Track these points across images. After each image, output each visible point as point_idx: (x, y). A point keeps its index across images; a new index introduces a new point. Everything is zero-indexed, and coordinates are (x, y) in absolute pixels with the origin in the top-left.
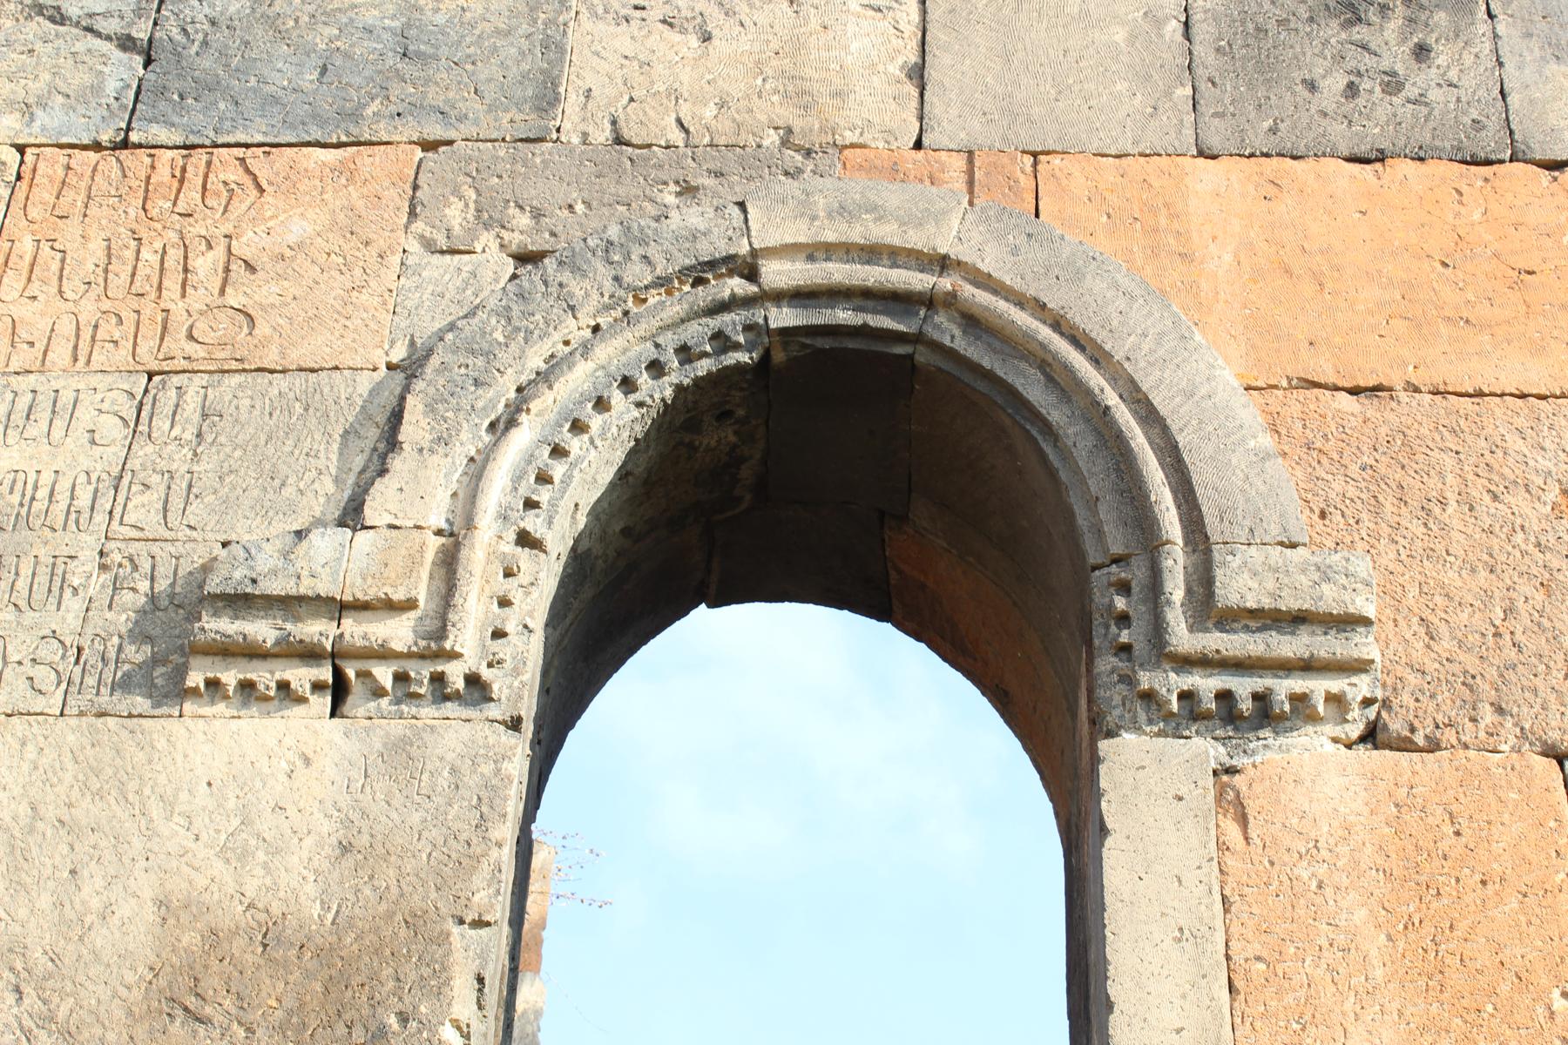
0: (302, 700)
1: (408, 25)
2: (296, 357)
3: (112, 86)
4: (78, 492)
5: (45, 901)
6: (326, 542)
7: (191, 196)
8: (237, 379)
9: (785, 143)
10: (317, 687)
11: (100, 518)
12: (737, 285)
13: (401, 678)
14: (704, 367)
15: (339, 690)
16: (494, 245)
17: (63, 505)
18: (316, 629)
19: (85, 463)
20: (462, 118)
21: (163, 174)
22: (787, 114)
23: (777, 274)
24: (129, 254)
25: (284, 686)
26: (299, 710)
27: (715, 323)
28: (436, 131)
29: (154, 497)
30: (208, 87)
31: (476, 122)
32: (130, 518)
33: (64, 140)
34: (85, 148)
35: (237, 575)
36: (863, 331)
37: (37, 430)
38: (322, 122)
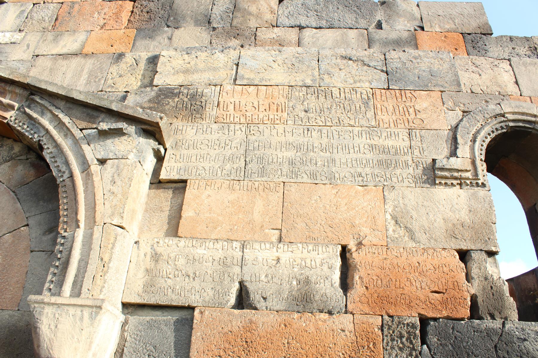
0: (455, 186)
1: (430, 70)
2: (433, 127)
3: (383, 79)
5: (424, 218)
6: (453, 159)
7: (404, 98)
8: (424, 131)
9: (499, 94)
10: (458, 184)
11: (410, 154)
12: (503, 119)
13: (471, 183)
14: (499, 132)
16: (458, 110)
18: (456, 174)
21: (398, 95)
22: (499, 89)
23: (510, 117)
24: (397, 108)
25: (452, 184)
26: (454, 188)
27: (501, 124)
28: (442, 89)
29: (418, 150)
35: (441, 164)
36: (525, 127)
37: (393, 138)
38: (422, 87)
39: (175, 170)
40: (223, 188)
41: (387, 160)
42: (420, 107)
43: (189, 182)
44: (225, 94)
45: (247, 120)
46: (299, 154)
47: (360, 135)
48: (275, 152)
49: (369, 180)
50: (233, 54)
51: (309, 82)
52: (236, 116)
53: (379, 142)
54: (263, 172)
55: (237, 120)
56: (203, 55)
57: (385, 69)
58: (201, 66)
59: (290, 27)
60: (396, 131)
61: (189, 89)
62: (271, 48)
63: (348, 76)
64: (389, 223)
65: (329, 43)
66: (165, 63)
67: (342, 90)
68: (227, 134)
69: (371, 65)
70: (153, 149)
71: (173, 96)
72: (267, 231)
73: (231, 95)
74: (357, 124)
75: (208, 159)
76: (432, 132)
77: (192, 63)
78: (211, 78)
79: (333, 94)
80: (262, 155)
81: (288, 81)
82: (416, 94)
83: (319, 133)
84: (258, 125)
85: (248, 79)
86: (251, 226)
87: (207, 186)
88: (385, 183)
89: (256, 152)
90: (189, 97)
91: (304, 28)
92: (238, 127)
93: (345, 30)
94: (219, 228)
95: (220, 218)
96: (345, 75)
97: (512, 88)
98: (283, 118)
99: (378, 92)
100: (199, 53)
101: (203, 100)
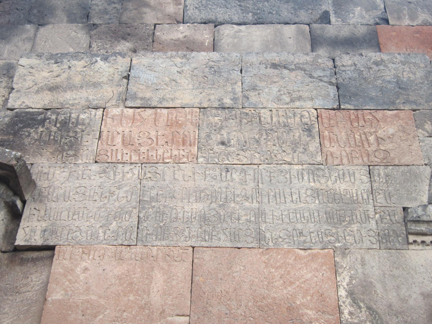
2: (403, 162)
3: (332, 95)
4: (363, 194)
7: (362, 123)
8: (391, 167)
11: (371, 201)
17: (361, 198)
19: (363, 188)
20: (420, 104)
21: (353, 117)
28: (415, 107)
30: (355, 95)
31: (424, 105)
32: (379, 201)
33: (326, 107)
34: (331, 109)
35: (415, 215)
37: (347, 179)
38: (388, 104)
39: (38, 232)
40: (106, 257)
41: (339, 211)
42: (385, 133)
43: (57, 249)
44: (109, 121)
45: (141, 158)
46: (214, 205)
47: (300, 177)
48: (180, 204)
49: (313, 241)
50: (122, 63)
51: (228, 101)
52: (125, 152)
53: (327, 186)
54: (163, 232)
55: (126, 158)
56: (79, 65)
57: (334, 80)
58: (77, 80)
59: (202, 23)
60: (352, 168)
61: (58, 114)
62: (174, 53)
63: (282, 93)
64: (344, 303)
65: (257, 45)
66: (25, 75)
67: (274, 111)
68: (112, 178)
69: (315, 75)
70: (6, 203)
71: (35, 124)
72: (169, 318)
73: (119, 124)
74: (296, 160)
75: (85, 216)
76: (402, 168)
77: (64, 76)
78: (91, 97)
79: (262, 119)
80: (161, 207)
81: (198, 100)
82: (379, 115)
83: (243, 175)
84: (157, 165)
85: (142, 99)
86: (147, 311)
87: (84, 255)
88: (337, 245)
89: (153, 204)
90: (58, 125)
91: (221, 24)
92: (127, 168)
93: (279, 26)
94: (101, 317)
95: (102, 302)
96: (279, 91)
98: (192, 155)
99: (325, 114)
100: (73, 62)
101: (78, 130)
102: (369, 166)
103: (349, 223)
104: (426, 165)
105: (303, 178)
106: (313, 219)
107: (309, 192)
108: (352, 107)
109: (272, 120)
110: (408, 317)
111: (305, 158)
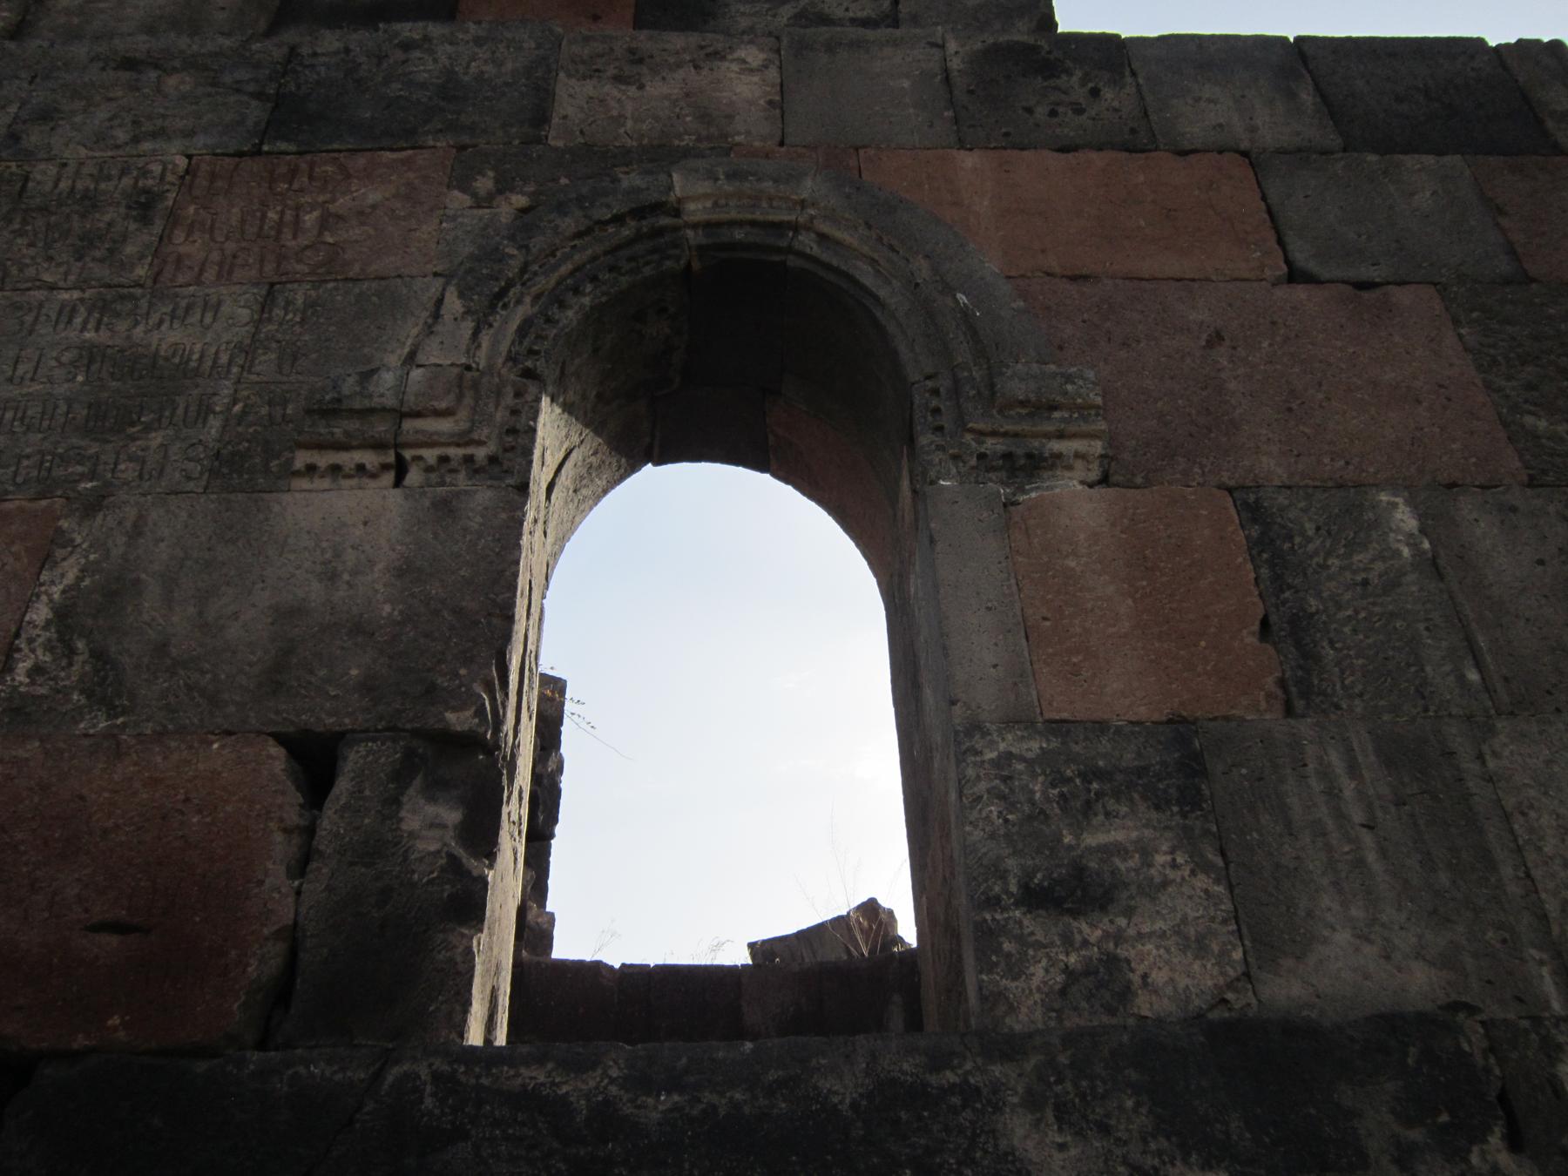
0: (374, 476)
10: (385, 467)
15: (401, 469)
18: (381, 428)
26: (372, 484)
47: (64, 319)
53: (128, 338)
63: (116, 122)
79: (30, 184)
82: (361, 161)
96: (110, 119)
97: (752, 127)
102: (272, 285)
103: (148, 428)
104: (436, 274)
105: (70, 322)
106: (46, 423)
107: (67, 357)
108: (292, 148)
109: (56, 185)
110: (203, 673)
111: (101, 272)
